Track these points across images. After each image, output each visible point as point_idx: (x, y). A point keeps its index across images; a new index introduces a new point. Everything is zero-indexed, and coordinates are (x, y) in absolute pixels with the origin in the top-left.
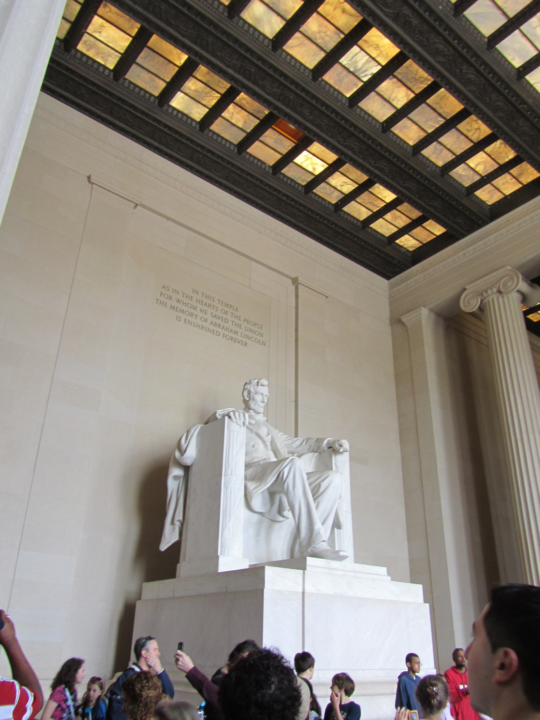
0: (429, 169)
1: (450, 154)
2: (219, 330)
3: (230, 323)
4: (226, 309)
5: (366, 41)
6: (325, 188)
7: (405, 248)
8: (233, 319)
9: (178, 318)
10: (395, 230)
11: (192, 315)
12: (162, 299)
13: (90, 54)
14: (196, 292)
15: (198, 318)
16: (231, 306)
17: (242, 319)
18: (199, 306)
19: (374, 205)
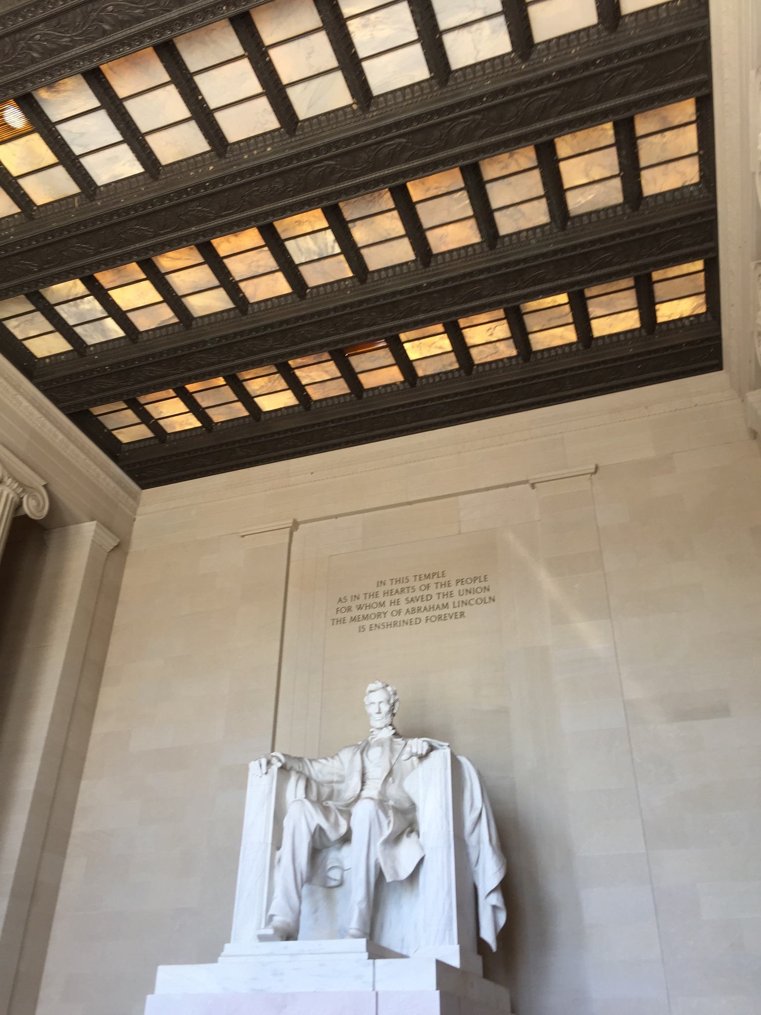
0: (533, 242)
1: (535, 203)
2: (420, 615)
3: (435, 597)
4: (426, 582)
5: (284, 231)
6: (481, 352)
7: (688, 317)
8: (440, 590)
9: (362, 629)
10: (635, 314)
11: (378, 615)
12: (340, 616)
13: (178, 429)
14: (383, 583)
15: (388, 615)
16: (434, 574)
17: (453, 583)
18: (388, 599)
19: (560, 317)
